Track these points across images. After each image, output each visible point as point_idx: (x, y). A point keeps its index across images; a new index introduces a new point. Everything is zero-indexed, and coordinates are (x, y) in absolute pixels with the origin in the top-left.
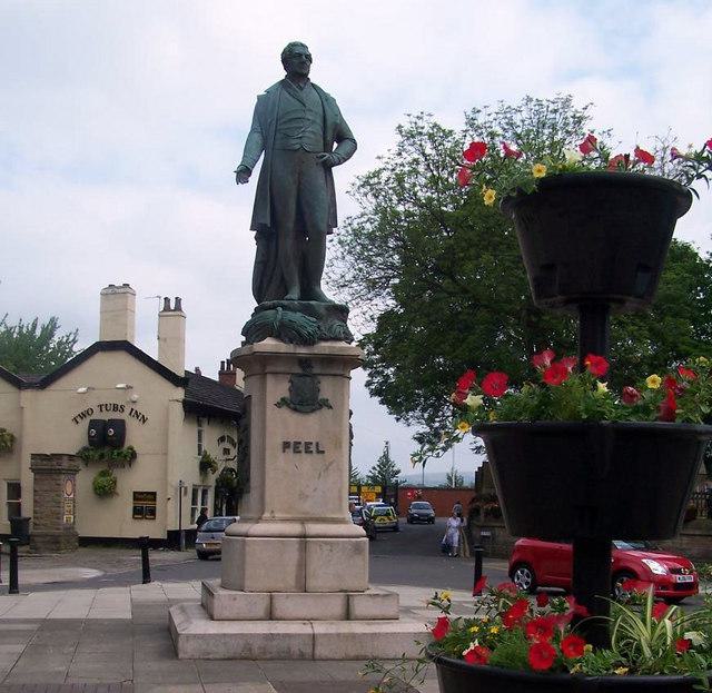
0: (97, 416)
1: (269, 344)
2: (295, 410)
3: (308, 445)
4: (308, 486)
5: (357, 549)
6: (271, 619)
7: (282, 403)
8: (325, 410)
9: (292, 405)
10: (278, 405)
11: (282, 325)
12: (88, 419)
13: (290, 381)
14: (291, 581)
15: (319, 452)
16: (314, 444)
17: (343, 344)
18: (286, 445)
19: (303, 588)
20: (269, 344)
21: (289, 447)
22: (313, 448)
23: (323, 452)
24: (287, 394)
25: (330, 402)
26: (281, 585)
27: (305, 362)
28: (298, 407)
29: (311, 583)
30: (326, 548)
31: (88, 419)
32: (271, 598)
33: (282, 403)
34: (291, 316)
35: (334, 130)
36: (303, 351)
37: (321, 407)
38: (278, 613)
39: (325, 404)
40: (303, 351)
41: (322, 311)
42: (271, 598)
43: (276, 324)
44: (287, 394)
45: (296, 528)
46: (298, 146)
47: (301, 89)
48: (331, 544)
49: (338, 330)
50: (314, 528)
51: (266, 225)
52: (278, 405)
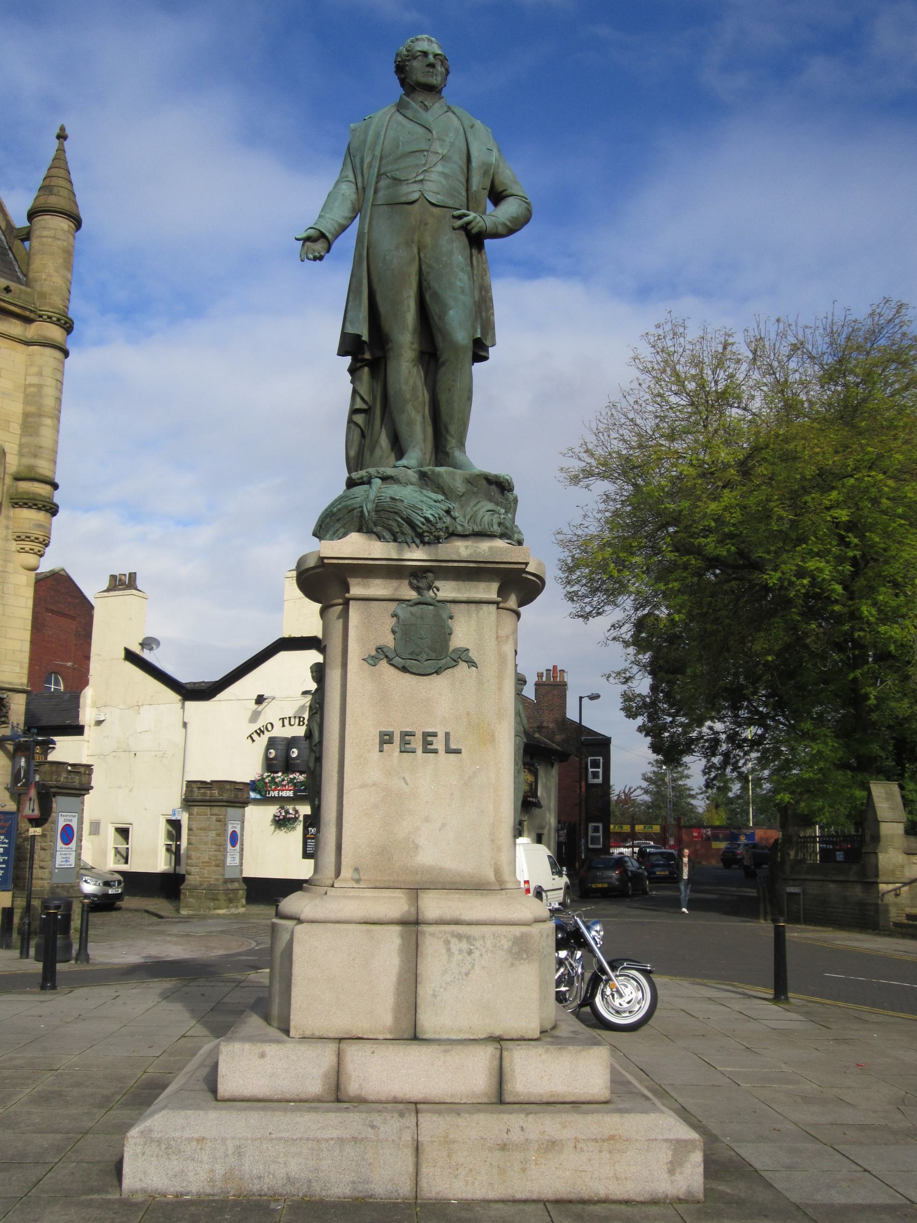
0: (280, 732)
1: (353, 546)
2: (404, 669)
3: (428, 737)
4: (427, 820)
5: (521, 949)
6: (338, 1101)
7: (381, 654)
8: (463, 666)
9: (398, 661)
10: (372, 660)
11: (380, 509)
12: (267, 735)
13: (394, 615)
14: (382, 1015)
15: (449, 751)
16: (441, 736)
17: (500, 543)
18: (386, 739)
19: (414, 1036)
20: (353, 546)
21: (390, 742)
22: (439, 743)
23: (458, 752)
24: (389, 641)
25: (473, 655)
26: (360, 1026)
27: (419, 576)
28: (408, 663)
29: (429, 1022)
30: (455, 945)
31: (267, 735)
32: (339, 1055)
33: (381, 654)
34: (393, 490)
35: (485, 173)
36: (417, 555)
37: (455, 662)
38: (353, 1087)
39: (463, 657)
40: (417, 555)
41: (460, 486)
42: (339, 1055)
43: (368, 507)
44: (389, 641)
45: (395, 905)
46: (415, 196)
47: (426, 109)
48: (468, 938)
49: (487, 518)
50: (433, 906)
51: (359, 337)
52: (372, 660)
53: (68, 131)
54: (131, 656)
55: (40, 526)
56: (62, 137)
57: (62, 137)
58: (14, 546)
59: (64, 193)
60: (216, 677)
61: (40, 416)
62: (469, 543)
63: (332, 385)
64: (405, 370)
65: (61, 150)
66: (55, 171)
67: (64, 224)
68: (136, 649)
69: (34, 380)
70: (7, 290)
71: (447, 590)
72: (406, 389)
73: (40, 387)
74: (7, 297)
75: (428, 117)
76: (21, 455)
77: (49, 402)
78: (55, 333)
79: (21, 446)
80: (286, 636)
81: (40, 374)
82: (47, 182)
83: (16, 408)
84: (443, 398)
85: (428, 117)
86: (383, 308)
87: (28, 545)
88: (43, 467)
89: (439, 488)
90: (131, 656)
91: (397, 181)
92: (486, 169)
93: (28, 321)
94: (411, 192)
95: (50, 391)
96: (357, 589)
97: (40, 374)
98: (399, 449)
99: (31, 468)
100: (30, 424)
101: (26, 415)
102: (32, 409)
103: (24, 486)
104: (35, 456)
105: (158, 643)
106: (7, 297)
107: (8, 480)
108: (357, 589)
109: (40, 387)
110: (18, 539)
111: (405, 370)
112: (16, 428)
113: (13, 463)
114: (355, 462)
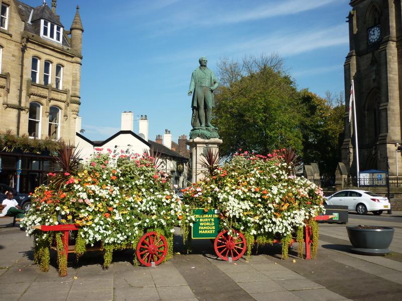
10: (200, 155)
36: (207, 141)
40: (207, 141)
52: (200, 155)
53: (79, 7)
54: (78, 134)
55: (77, 108)
58: (72, 113)
59: (80, 24)
60: (105, 140)
61: (76, 81)
62: (213, 139)
63: (189, 112)
64: (202, 111)
65: (78, 12)
66: (77, 18)
67: (80, 32)
68: (79, 133)
69: (74, 72)
70: (68, 49)
71: (210, 146)
72: (202, 114)
73: (76, 74)
74: (68, 51)
75: (205, 71)
76: (72, 90)
78: (79, 60)
79: (72, 88)
80: (122, 130)
81: (76, 70)
82: (75, 21)
83: (71, 79)
84: (207, 115)
85: (205, 71)
86: (199, 102)
87: (75, 113)
88: (78, 94)
89: (209, 131)
90: (78, 134)
91: (201, 83)
92: (214, 80)
93: (72, 57)
94: (204, 85)
96: (198, 145)
97: (76, 70)
98: (201, 124)
99: (75, 94)
101: (73, 81)
102: (74, 79)
103: (73, 98)
104: (76, 91)
105: (84, 130)
106: (68, 51)
107: (70, 97)
108: (198, 145)
109: (76, 74)
111: (202, 111)
112: (71, 84)
113: (71, 93)
114: (193, 125)
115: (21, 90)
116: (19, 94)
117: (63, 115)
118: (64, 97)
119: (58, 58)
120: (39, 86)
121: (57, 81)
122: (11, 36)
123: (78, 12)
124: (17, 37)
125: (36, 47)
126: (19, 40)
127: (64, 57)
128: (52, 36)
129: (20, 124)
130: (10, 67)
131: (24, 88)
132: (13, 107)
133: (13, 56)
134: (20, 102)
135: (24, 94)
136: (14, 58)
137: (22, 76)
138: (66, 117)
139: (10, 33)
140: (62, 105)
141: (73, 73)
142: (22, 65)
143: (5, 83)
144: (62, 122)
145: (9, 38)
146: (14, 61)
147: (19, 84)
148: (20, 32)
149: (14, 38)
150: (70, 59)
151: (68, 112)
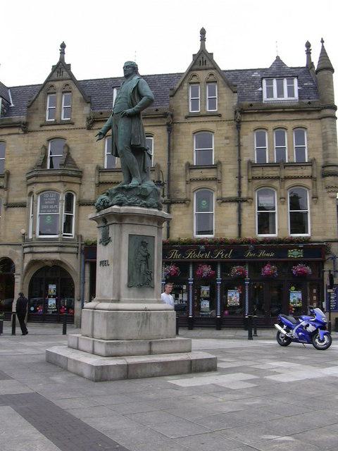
56: (322, 42)
57: (322, 42)
58: (325, 191)
61: (327, 142)
65: (323, 47)
77: (330, 137)
79: (323, 155)
83: (319, 142)
95: (330, 133)
97: (325, 128)
100: (325, 147)
101: (323, 144)
102: (325, 141)
103: (326, 169)
110: (326, 188)
112: (321, 150)
113: (320, 162)
115: (240, 177)
116: (237, 183)
117: (311, 196)
118: (307, 171)
119: (294, 120)
120: (271, 165)
121: (300, 151)
122: (220, 115)
123: (323, 47)
124: (228, 114)
125: (258, 117)
126: (232, 116)
127: (305, 116)
128: (280, 93)
129: (242, 220)
130: (223, 152)
131: (244, 173)
132: (230, 200)
133: (227, 138)
134: (240, 193)
135: (244, 181)
136: (228, 141)
137: (240, 160)
138: (314, 199)
139: (219, 113)
140: (308, 183)
141: (323, 133)
142: (239, 146)
143: (215, 174)
144: (311, 208)
145: (218, 119)
146: (228, 144)
147: (237, 171)
148: (231, 108)
149: (225, 117)
150: (316, 115)
151: (320, 191)
